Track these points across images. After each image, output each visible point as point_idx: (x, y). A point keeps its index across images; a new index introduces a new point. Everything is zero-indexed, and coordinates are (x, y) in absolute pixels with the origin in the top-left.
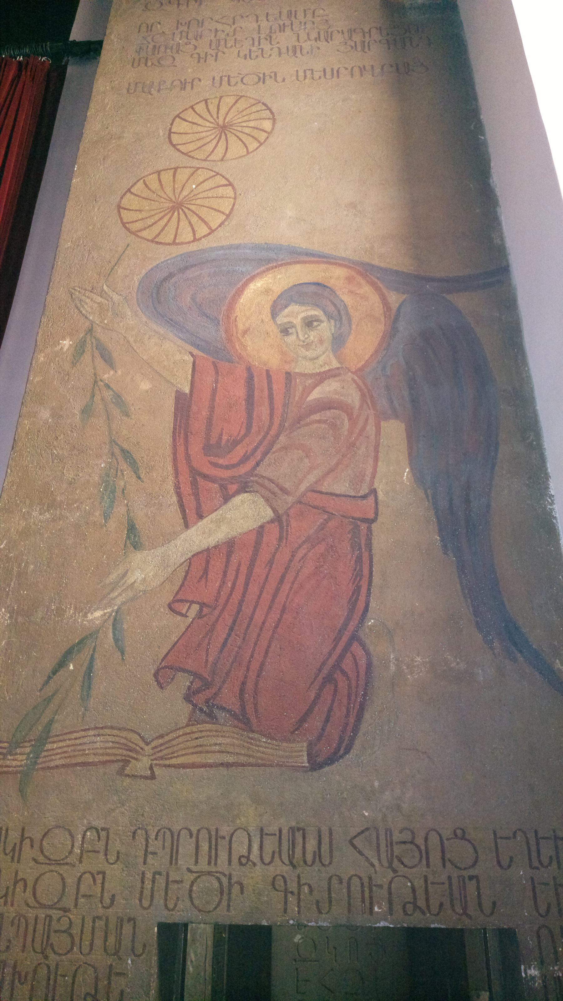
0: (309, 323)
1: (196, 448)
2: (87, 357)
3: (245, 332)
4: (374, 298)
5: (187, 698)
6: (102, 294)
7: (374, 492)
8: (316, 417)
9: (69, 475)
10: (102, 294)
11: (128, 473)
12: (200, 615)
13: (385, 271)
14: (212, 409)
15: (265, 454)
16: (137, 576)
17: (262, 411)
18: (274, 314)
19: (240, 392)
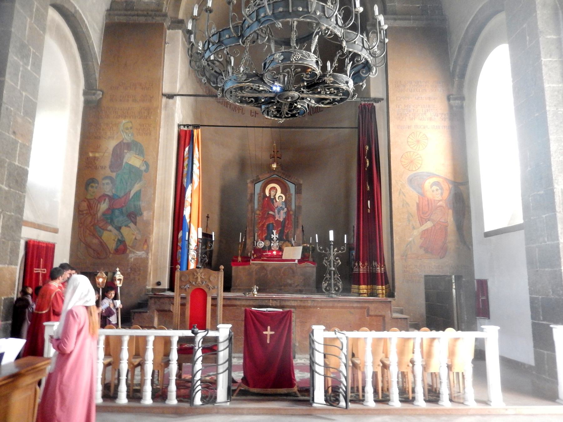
0: (437, 190)
1: (421, 213)
2: (401, 195)
3: (426, 191)
4: (447, 186)
5: (424, 250)
6: (401, 181)
7: (447, 222)
8: (439, 208)
9: (402, 217)
10: (401, 181)
11: (411, 217)
12: (424, 240)
13: (449, 180)
14: (422, 206)
15: (431, 215)
16: (415, 234)
17: (430, 207)
18: (431, 187)
19: (427, 203)
